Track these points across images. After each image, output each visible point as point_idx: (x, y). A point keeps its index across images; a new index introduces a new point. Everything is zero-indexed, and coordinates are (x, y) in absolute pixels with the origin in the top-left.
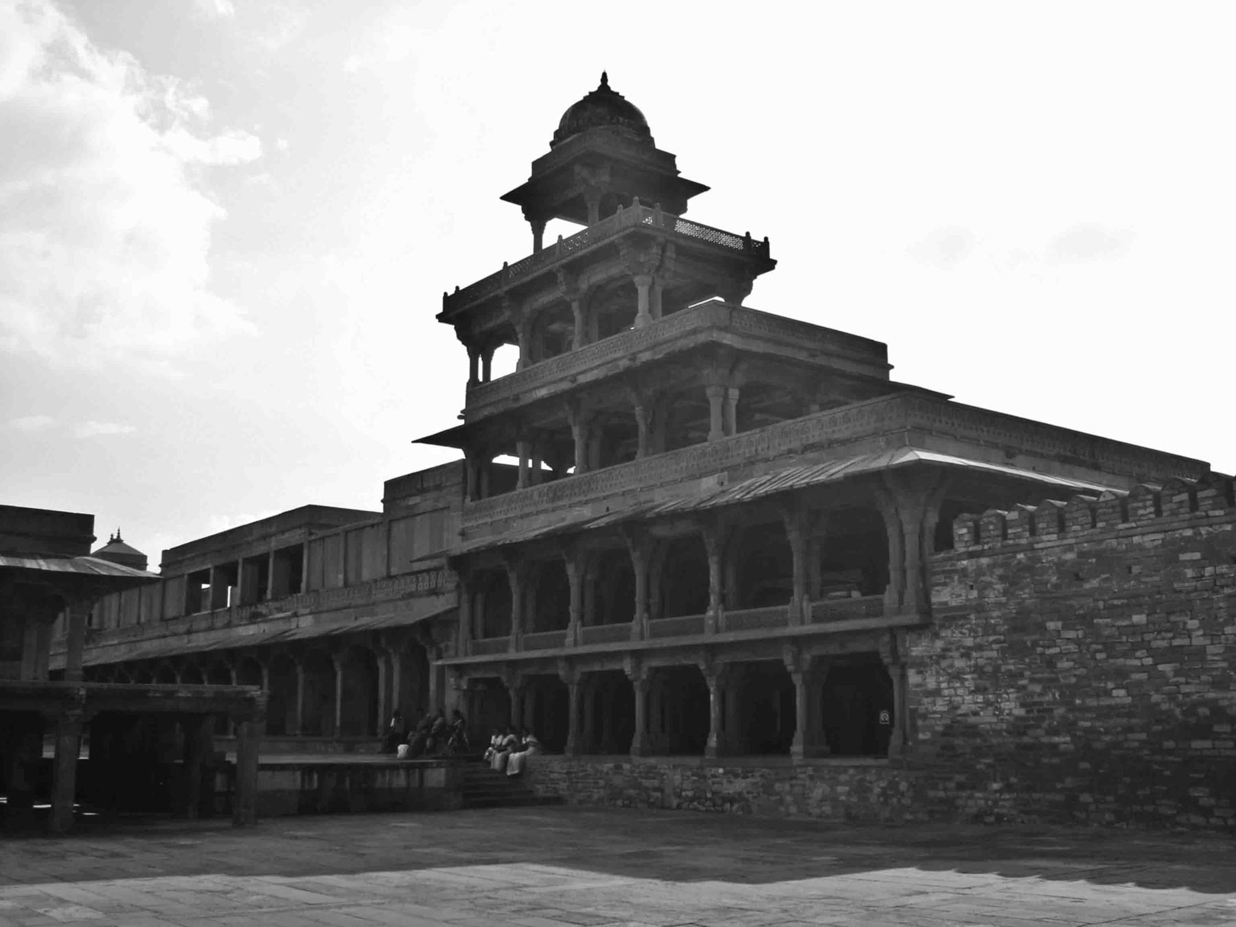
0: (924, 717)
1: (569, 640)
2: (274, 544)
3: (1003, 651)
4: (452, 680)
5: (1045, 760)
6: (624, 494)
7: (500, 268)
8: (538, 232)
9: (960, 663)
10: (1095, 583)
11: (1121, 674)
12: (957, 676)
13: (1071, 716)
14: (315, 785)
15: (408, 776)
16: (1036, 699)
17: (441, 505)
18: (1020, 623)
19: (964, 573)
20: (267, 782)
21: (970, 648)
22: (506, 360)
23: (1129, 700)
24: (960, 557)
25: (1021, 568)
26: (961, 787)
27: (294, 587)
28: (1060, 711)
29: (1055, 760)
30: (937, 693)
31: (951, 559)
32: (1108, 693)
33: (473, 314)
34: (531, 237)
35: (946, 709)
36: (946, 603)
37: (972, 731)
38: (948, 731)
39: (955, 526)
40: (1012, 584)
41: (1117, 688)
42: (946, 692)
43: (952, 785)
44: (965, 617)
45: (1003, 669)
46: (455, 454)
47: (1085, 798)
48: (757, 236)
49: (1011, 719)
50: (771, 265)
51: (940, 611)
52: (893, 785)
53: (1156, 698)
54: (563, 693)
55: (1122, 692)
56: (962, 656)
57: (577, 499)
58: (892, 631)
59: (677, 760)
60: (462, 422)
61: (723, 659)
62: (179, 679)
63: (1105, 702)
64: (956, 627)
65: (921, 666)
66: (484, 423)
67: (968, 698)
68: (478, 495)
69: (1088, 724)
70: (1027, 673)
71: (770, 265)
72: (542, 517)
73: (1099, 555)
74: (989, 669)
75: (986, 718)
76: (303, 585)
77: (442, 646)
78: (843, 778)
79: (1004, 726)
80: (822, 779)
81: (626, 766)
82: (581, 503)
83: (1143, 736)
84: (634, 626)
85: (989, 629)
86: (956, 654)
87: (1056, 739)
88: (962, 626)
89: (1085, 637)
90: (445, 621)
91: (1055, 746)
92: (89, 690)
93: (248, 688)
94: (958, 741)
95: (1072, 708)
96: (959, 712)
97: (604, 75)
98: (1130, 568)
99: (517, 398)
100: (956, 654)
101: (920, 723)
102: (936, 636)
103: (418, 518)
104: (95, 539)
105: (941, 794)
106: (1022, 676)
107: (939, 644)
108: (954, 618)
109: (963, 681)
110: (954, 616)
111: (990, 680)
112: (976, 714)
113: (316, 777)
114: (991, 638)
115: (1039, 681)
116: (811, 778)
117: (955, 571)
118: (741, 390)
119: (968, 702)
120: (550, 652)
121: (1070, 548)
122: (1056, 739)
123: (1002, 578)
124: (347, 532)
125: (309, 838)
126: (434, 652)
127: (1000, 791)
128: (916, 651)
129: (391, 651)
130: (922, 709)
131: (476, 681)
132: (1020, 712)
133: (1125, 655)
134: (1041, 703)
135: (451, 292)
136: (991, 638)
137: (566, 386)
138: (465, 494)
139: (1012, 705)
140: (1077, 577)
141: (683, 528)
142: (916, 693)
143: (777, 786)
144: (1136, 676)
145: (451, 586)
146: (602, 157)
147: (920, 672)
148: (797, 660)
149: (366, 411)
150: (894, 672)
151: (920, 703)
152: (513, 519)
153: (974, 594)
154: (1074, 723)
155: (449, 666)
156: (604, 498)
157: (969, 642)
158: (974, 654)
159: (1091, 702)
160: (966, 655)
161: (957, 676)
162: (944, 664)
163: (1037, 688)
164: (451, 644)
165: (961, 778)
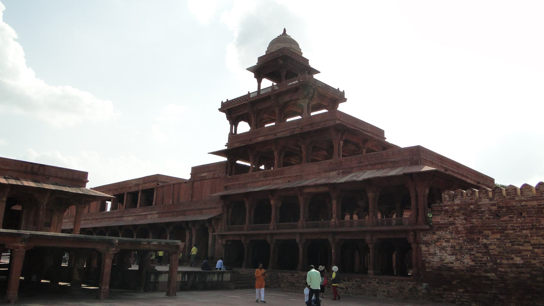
0: (429, 263)
2: (141, 188)
3: (464, 241)
4: (220, 240)
5: (484, 282)
6: (296, 176)
7: (247, 93)
8: (259, 82)
9: (444, 244)
10: (506, 218)
11: (518, 253)
12: (443, 249)
13: (495, 266)
14: (186, 280)
15: (218, 277)
16: (479, 259)
17: (216, 176)
18: (471, 231)
19: (447, 211)
21: (449, 239)
23: (522, 262)
24: (445, 206)
25: (472, 211)
26: (445, 290)
28: (491, 264)
29: (488, 282)
30: (435, 254)
31: (442, 206)
32: (512, 259)
33: (234, 110)
34: (257, 84)
35: (439, 260)
36: (439, 222)
37: (450, 269)
39: (443, 195)
40: (468, 216)
41: (517, 256)
42: (439, 254)
43: (441, 289)
44: (447, 227)
45: (464, 247)
46: (225, 159)
47: (501, 297)
48: (341, 90)
49: (468, 266)
50: (345, 100)
51: (436, 224)
53: (533, 262)
55: (519, 259)
56: (446, 241)
57: (277, 177)
58: (415, 232)
60: (226, 148)
62: (151, 236)
63: (511, 262)
64: (443, 230)
65: (427, 244)
66: (236, 148)
67: (448, 257)
69: (503, 270)
70: (475, 249)
71: (345, 100)
72: (260, 183)
73: (506, 207)
75: (457, 265)
76: (154, 203)
77: (215, 227)
78: (392, 283)
79: (465, 268)
80: (382, 283)
81: (296, 275)
82: (277, 179)
83: (529, 275)
84: (299, 224)
85: (458, 232)
86: (444, 241)
87: (489, 274)
88: (446, 231)
89: (501, 236)
90: (217, 219)
91: (488, 277)
92: (119, 240)
93: (177, 241)
95: (496, 263)
96: (445, 262)
97: (285, 29)
98: (521, 214)
99: (250, 140)
100: (444, 241)
101: (427, 265)
102: (434, 233)
103: (205, 181)
104: (88, 181)
105: (438, 292)
106: (472, 250)
107: (435, 237)
108: (442, 227)
109: (446, 251)
110: (442, 227)
112: (452, 263)
113: (187, 276)
114: (459, 236)
115: (481, 252)
116: (378, 283)
117: (443, 211)
118: (344, 142)
120: (265, 232)
121: (494, 205)
122: (489, 274)
123: (463, 214)
125: (206, 303)
126: (211, 230)
127: (463, 292)
128: (425, 239)
129: (193, 229)
130: (428, 260)
131: (229, 241)
132: (473, 263)
133: (519, 245)
134: (482, 261)
135: (225, 101)
136: (459, 236)
137: (274, 137)
138: (226, 173)
139: (469, 261)
140: (497, 216)
142: (426, 254)
143: (363, 285)
144: (524, 253)
147: (426, 246)
150: (414, 246)
151: (427, 257)
152: (249, 183)
153: (452, 219)
155: (218, 235)
156: (288, 177)
157: (449, 236)
158: (451, 240)
159: (504, 262)
160: (448, 241)
161: (443, 249)
162: (438, 244)
163: (480, 255)
164: (219, 227)
165: (446, 287)
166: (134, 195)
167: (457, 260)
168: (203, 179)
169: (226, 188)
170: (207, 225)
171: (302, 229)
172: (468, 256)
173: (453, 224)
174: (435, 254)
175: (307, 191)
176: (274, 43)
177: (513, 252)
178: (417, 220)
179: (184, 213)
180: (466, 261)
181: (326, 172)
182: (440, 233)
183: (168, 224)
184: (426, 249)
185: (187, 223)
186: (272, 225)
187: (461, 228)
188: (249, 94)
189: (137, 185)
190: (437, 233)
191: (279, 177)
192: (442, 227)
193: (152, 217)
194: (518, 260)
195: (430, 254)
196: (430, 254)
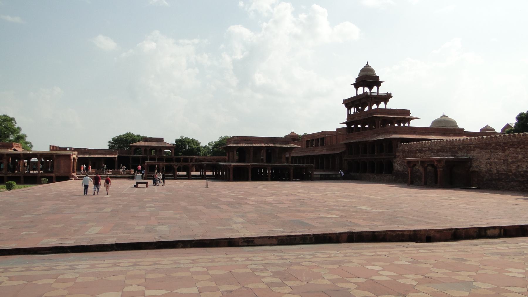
20: (315, 176)
22: (352, 110)
27: (323, 145)
37: (399, 171)
46: (345, 126)
48: (389, 92)
50: (392, 97)
66: (351, 121)
68: (349, 133)
71: (392, 97)
75: (400, 170)
90: (344, 153)
111: (401, 165)
146: (367, 78)
149: (332, 118)
166: (318, 140)
168: (340, 134)
176: (362, 71)
179: (334, 150)
183: (329, 154)
188: (352, 98)
189: (318, 136)
193: (323, 151)
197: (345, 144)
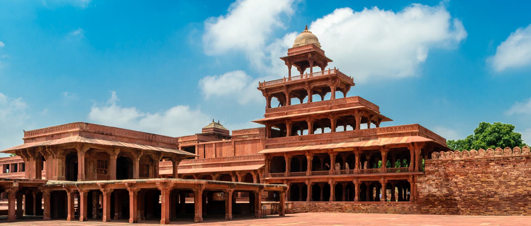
0: (421, 193)
1: (307, 174)
9: (432, 182)
12: (431, 185)
28: (458, 192)
32: (470, 189)
37: (434, 196)
38: (428, 196)
52: (412, 207)
53: (481, 190)
54: (306, 186)
59: (346, 202)
61: (360, 180)
63: (469, 191)
65: (421, 182)
67: (434, 189)
72: (296, 144)
74: (439, 184)
75: (438, 194)
77: (260, 175)
82: (312, 142)
84: (330, 171)
85: (440, 176)
90: (261, 169)
94: (431, 199)
101: (420, 194)
102: (426, 176)
107: (426, 179)
110: (430, 173)
119: (434, 190)
124: (215, 143)
126: (256, 176)
128: (419, 180)
129: (239, 176)
130: (421, 191)
132: (448, 192)
141: (352, 149)
145: (263, 159)
148: (384, 180)
150: (412, 184)
154: (461, 195)
157: (435, 178)
160: (434, 181)
161: (431, 185)
162: (428, 182)
167: (439, 191)
169: (267, 147)
170: (253, 173)
171: (334, 176)
172: (445, 189)
173: (438, 171)
174: (425, 188)
175: (335, 150)
177: (470, 186)
178: (414, 169)
180: (444, 191)
181: (350, 138)
182: (430, 176)
184: (420, 185)
185: (234, 172)
186: (309, 172)
187: (442, 173)
190: (427, 176)
191: (313, 140)
192: (430, 173)
194: (473, 190)
195: (422, 188)
196: (422, 188)
197: (266, 155)
